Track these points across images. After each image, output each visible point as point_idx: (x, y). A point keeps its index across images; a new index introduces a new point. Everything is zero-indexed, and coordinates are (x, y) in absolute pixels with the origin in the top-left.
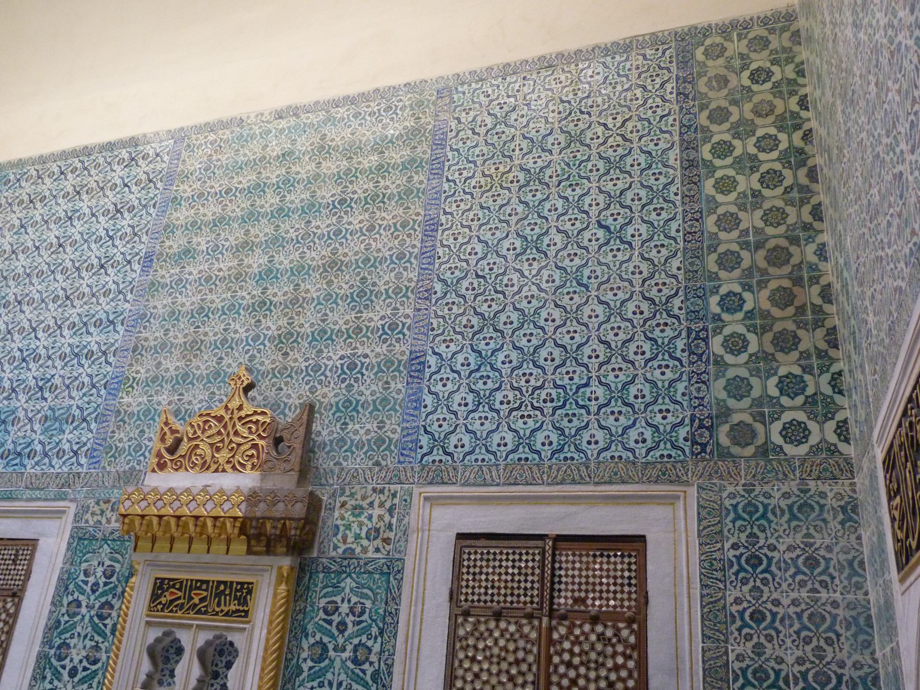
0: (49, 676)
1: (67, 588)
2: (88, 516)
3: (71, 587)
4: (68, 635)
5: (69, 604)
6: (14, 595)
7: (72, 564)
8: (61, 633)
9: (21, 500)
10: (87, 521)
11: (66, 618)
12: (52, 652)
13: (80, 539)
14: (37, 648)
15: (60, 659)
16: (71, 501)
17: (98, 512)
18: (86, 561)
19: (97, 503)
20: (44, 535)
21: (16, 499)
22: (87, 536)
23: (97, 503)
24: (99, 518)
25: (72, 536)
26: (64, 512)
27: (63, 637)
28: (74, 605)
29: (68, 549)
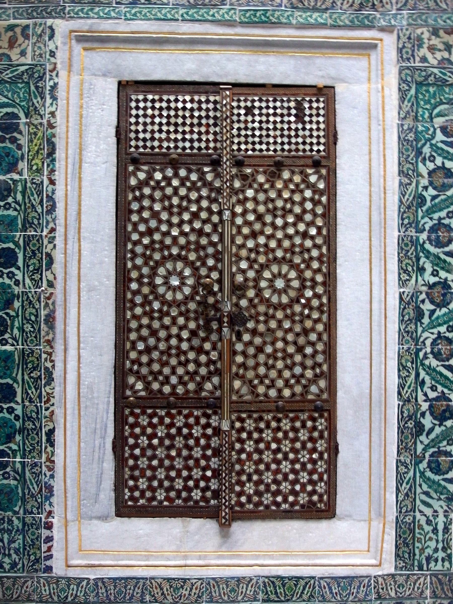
0: (429, 268)
1: (419, 152)
2: (424, 51)
3: (427, 150)
4: (443, 214)
5: (430, 173)
6: (316, 164)
7: (416, 119)
8: (429, 213)
9: (288, 25)
10: (424, 59)
11: (432, 191)
12: (424, 236)
13: (419, 84)
14: (394, 235)
15: (439, 244)
16: (382, 29)
17: (441, 46)
18: (440, 115)
19: (435, 33)
20: (343, 81)
21: (278, 24)
22: (431, 80)
23: (435, 33)
24: (446, 55)
25: (402, 80)
26: (375, 46)
27: (436, 216)
28: (440, 174)
29: (402, 99)
